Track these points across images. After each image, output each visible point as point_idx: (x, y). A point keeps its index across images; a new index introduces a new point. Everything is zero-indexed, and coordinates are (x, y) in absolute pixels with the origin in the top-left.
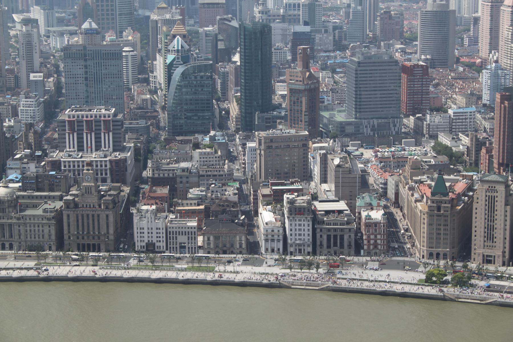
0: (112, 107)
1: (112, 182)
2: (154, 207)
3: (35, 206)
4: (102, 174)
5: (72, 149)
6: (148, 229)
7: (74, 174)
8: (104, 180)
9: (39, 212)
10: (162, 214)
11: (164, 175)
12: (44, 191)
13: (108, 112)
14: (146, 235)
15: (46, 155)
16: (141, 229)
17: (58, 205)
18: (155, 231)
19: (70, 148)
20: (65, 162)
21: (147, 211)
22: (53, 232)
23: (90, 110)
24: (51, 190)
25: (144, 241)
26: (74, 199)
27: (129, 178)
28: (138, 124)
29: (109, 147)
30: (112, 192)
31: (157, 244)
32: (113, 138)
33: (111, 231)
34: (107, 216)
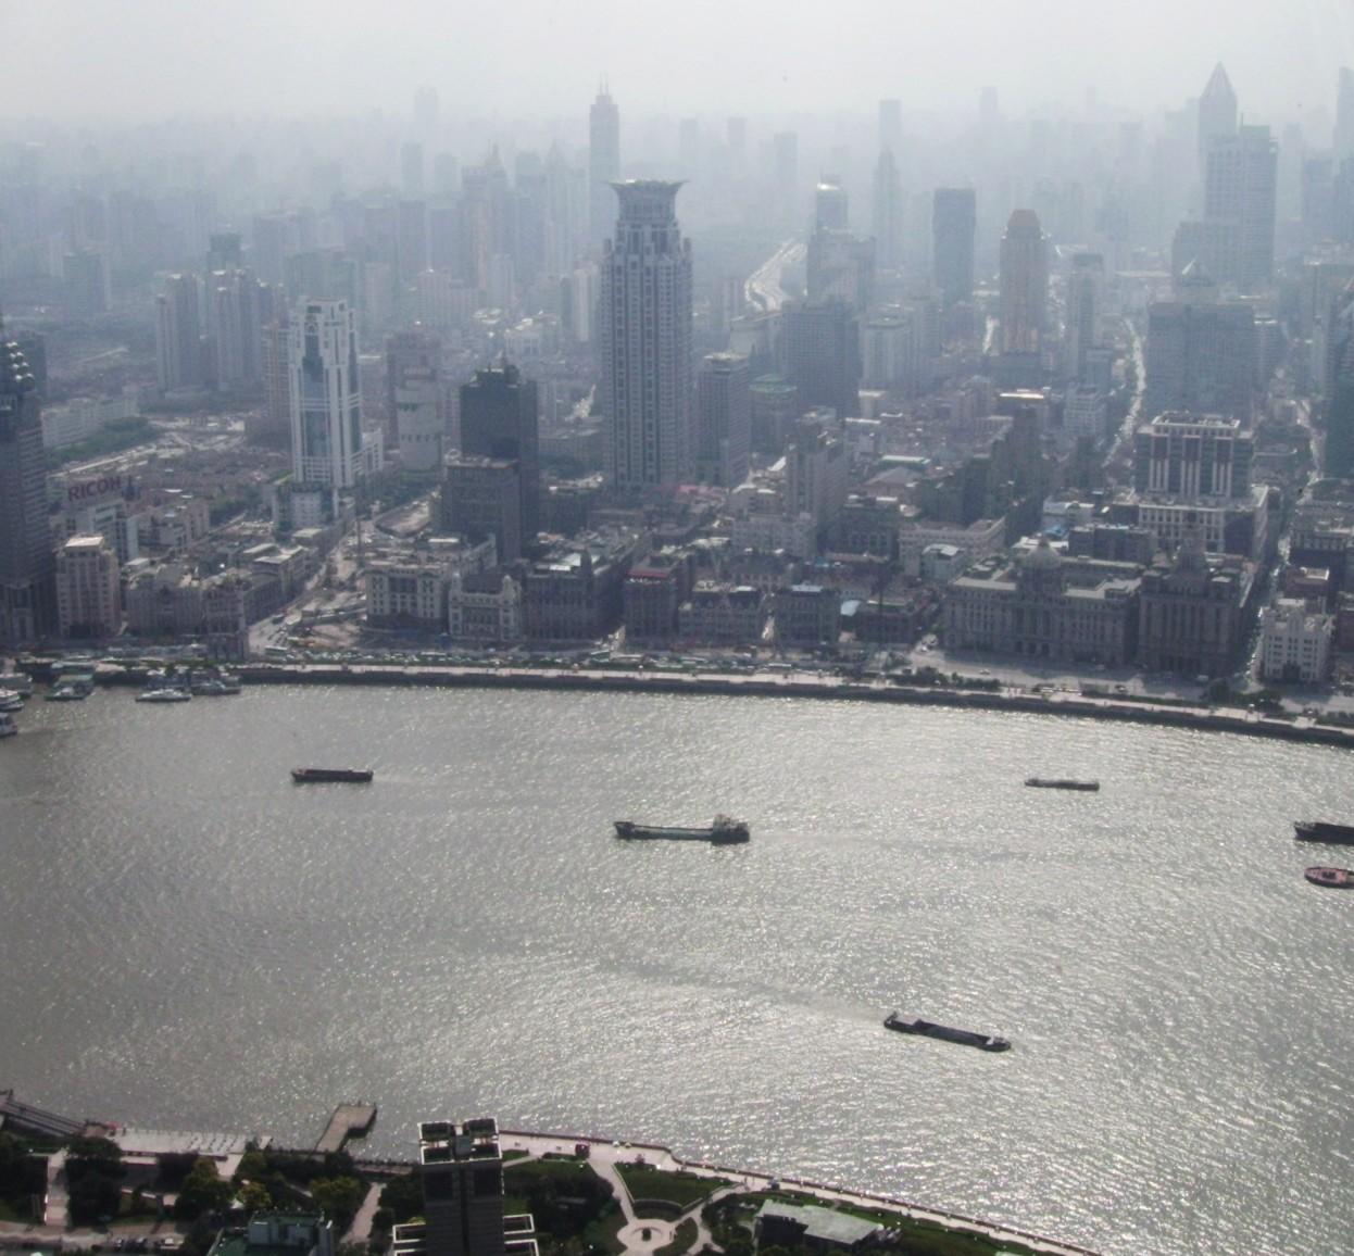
0: (1236, 418)
1: (1228, 551)
2: (1301, 602)
3: (1091, 585)
4: (1209, 537)
5: (1157, 489)
6: (1290, 640)
7: (1160, 533)
8: (1212, 547)
9: (1098, 594)
10: (1318, 616)
11: (1321, 546)
12: (1105, 558)
13: (1227, 426)
14: (1285, 651)
15: (1110, 496)
16: (1276, 639)
17: (1132, 585)
18: (1301, 645)
19: (1155, 486)
20: (1145, 510)
21: (1290, 608)
22: (1120, 632)
23: (1195, 421)
24: (1120, 557)
25: (1279, 662)
26: (1160, 577)
27: (1259, 548)
28: (1274, 450)
29: (1225, 487)
30: (1229, 570)
31: (1305, 669)
32: (1233, 472)
33: (1224, 638)
34: (1218, 613)
